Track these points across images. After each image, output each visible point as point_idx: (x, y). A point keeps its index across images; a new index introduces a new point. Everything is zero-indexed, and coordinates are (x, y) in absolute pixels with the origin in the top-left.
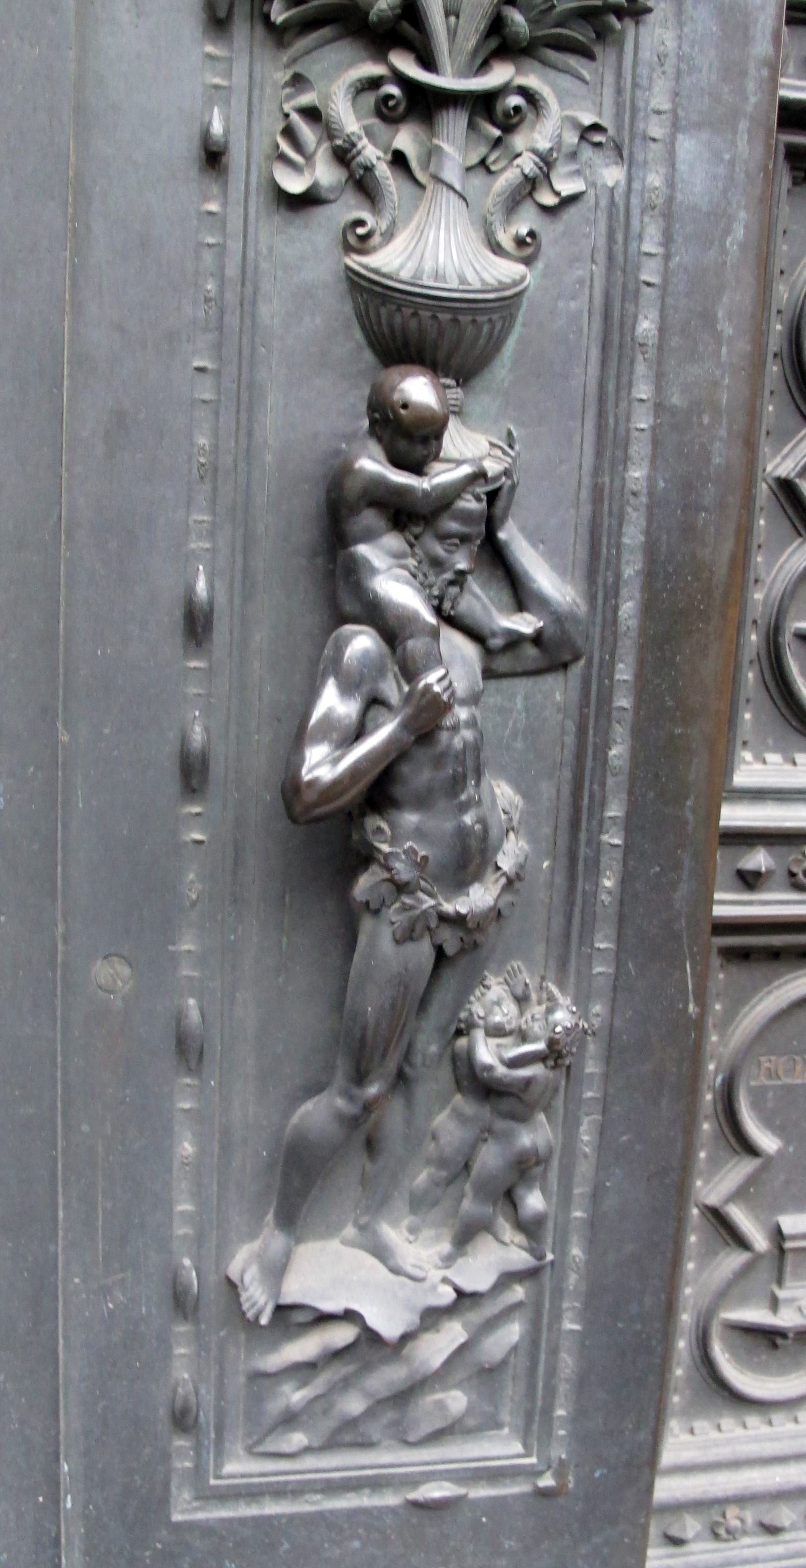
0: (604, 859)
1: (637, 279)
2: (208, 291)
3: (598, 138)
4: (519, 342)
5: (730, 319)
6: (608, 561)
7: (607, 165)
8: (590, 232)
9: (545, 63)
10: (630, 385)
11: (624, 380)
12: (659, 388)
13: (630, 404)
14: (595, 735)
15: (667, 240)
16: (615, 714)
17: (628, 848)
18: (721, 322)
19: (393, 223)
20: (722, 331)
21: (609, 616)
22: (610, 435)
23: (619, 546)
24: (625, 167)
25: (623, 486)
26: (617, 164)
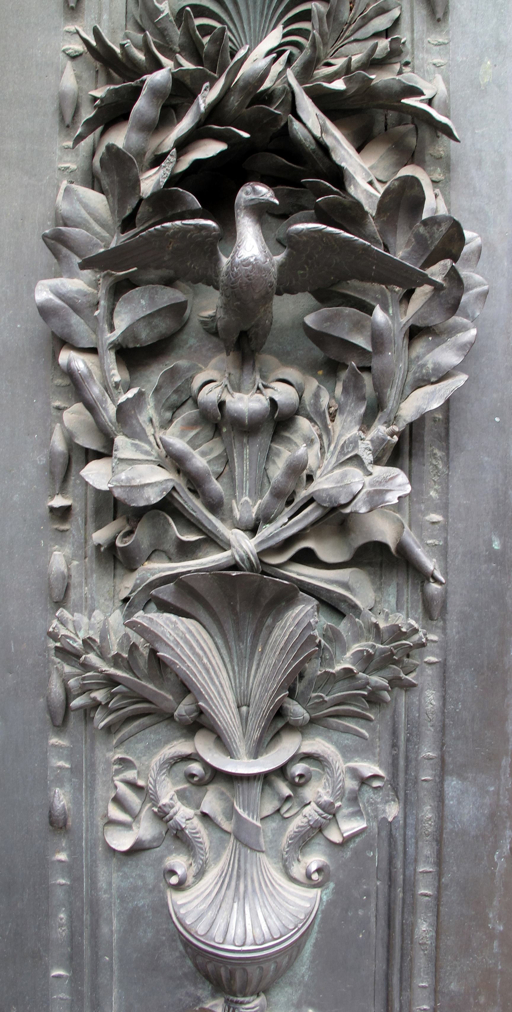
2: (61, 919)
3: (376, 784)
5: (500, 919)
7: (387, 802)
8: (374, 856)
9: (329, 727)
10: (411, 977)
15: (439, 862)
18: (492, 921)
19: (205, 863)
20: (493, 929)
24: (402, 804)
26: (394, 801)
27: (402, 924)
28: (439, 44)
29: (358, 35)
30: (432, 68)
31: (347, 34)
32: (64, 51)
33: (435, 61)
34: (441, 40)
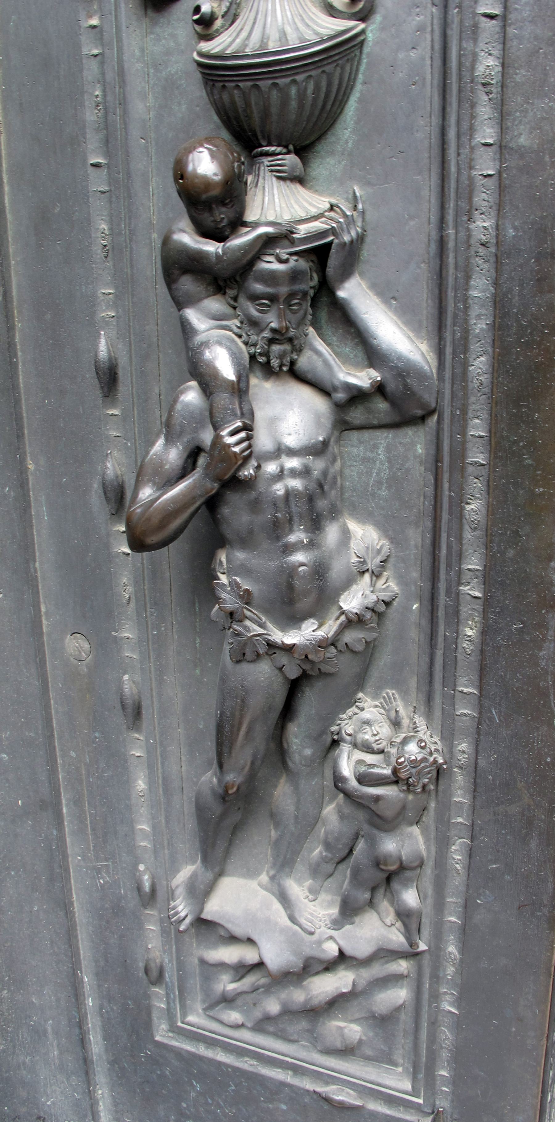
0: (465, 610)
1: (475, 14)
2: (97, 96)
4: (360, 101)
6: (455, 316)
11: (465, 125)
12: (502, 129)
13: (472, 149)
14: (450, 490)
16: (470, 469)
17: (487, 602)
21: (458, 371)
22: (453, 184)
23: (465, 299)
25: (469, 236)
27: (460, 56)
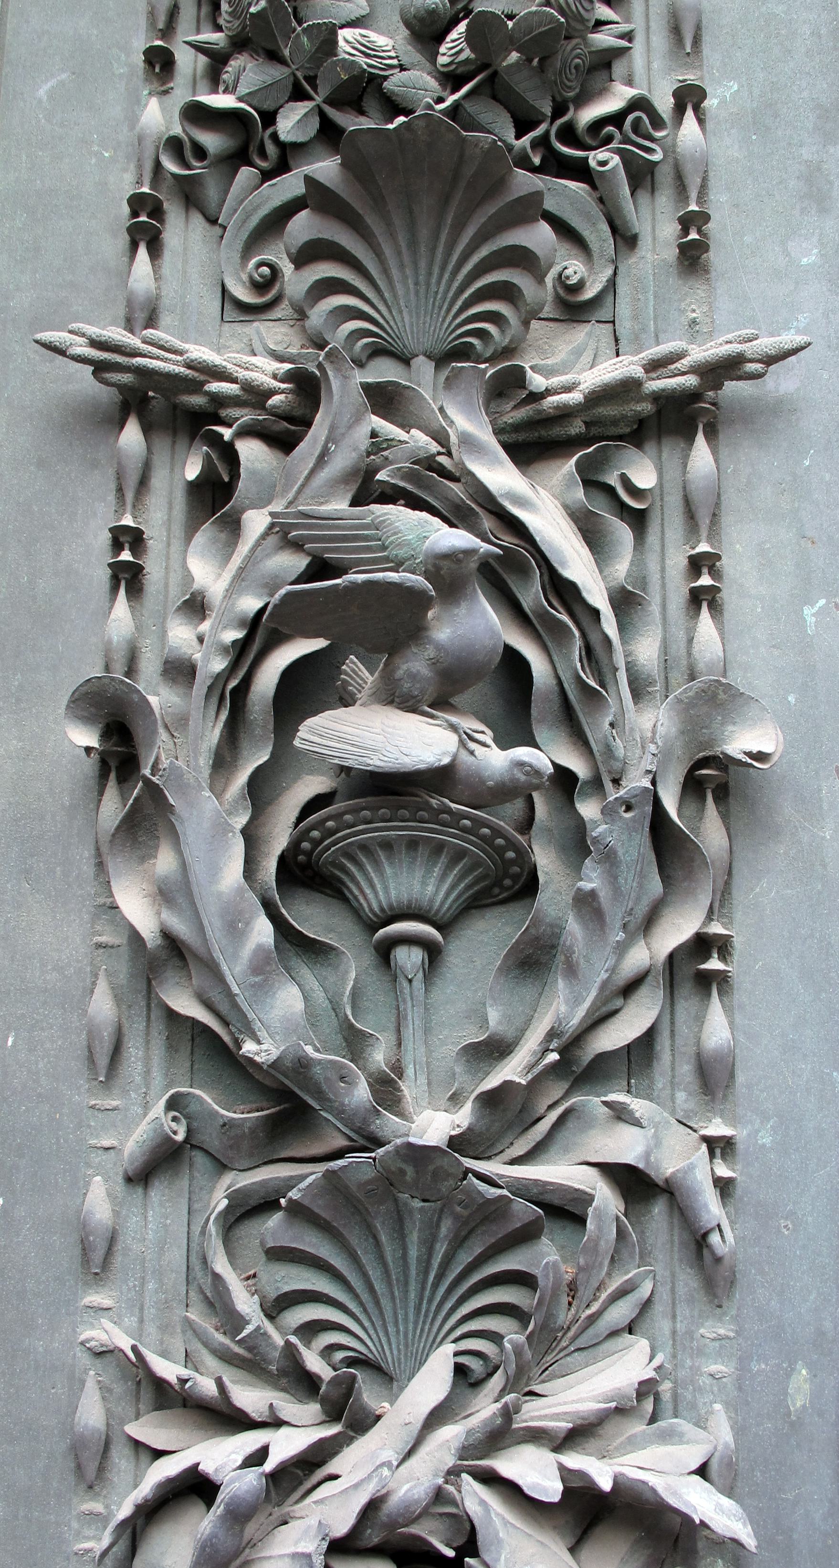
28: (720, 1338)
29: (581, 1342)
30: (708, 1381)
31: (564, 1344)
32: (82, 1343)
33: (714, 1368)
34: (722, 1331)
